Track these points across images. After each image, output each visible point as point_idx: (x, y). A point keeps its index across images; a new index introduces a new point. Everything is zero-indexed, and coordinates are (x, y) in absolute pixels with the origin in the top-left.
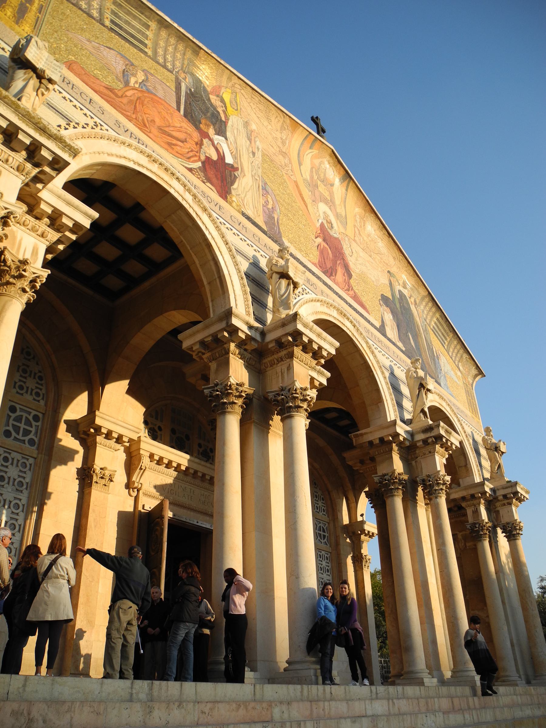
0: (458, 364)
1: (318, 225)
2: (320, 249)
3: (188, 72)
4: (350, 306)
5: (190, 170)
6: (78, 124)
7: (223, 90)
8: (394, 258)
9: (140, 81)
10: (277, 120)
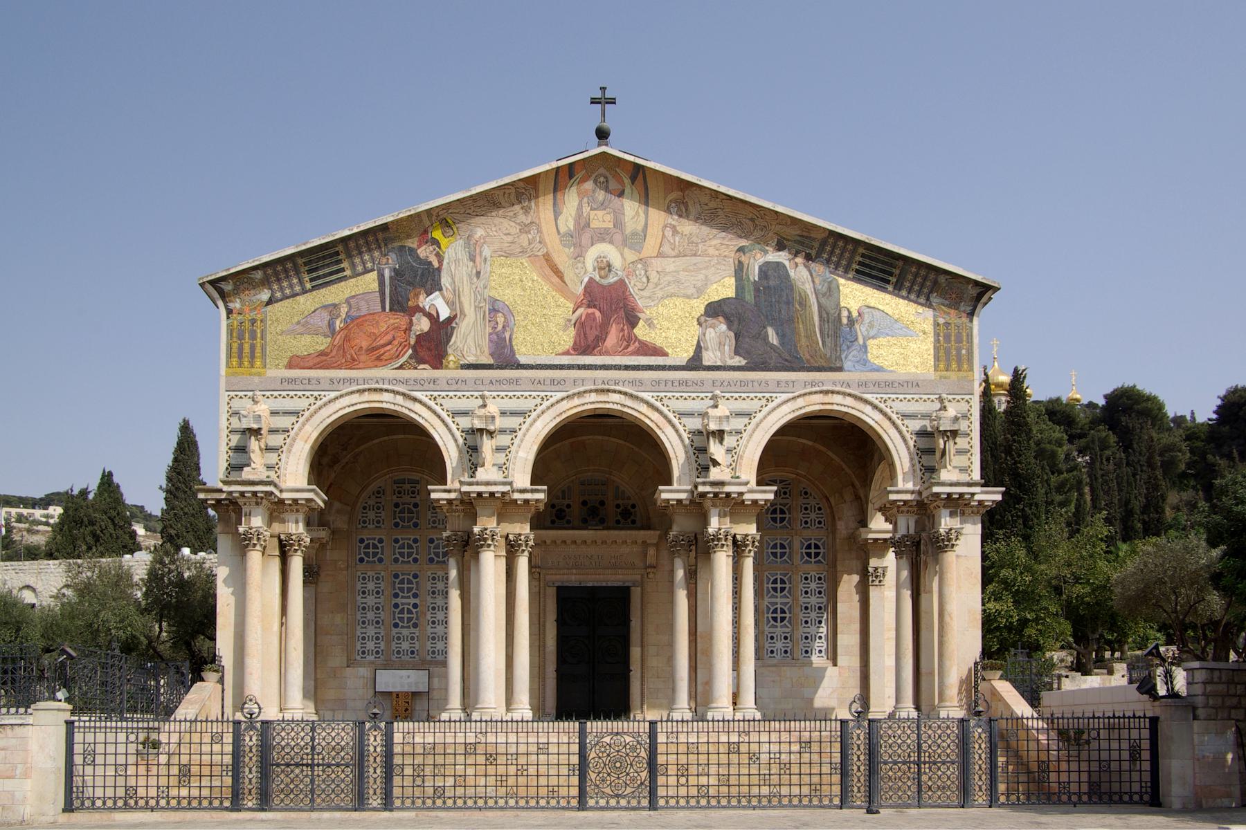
1: (580, 290)
2: (580, 323)
4: (627, 368)
5: (401, 367)
6: (304, 411)
8: (752, 220)
9: (344, 316)
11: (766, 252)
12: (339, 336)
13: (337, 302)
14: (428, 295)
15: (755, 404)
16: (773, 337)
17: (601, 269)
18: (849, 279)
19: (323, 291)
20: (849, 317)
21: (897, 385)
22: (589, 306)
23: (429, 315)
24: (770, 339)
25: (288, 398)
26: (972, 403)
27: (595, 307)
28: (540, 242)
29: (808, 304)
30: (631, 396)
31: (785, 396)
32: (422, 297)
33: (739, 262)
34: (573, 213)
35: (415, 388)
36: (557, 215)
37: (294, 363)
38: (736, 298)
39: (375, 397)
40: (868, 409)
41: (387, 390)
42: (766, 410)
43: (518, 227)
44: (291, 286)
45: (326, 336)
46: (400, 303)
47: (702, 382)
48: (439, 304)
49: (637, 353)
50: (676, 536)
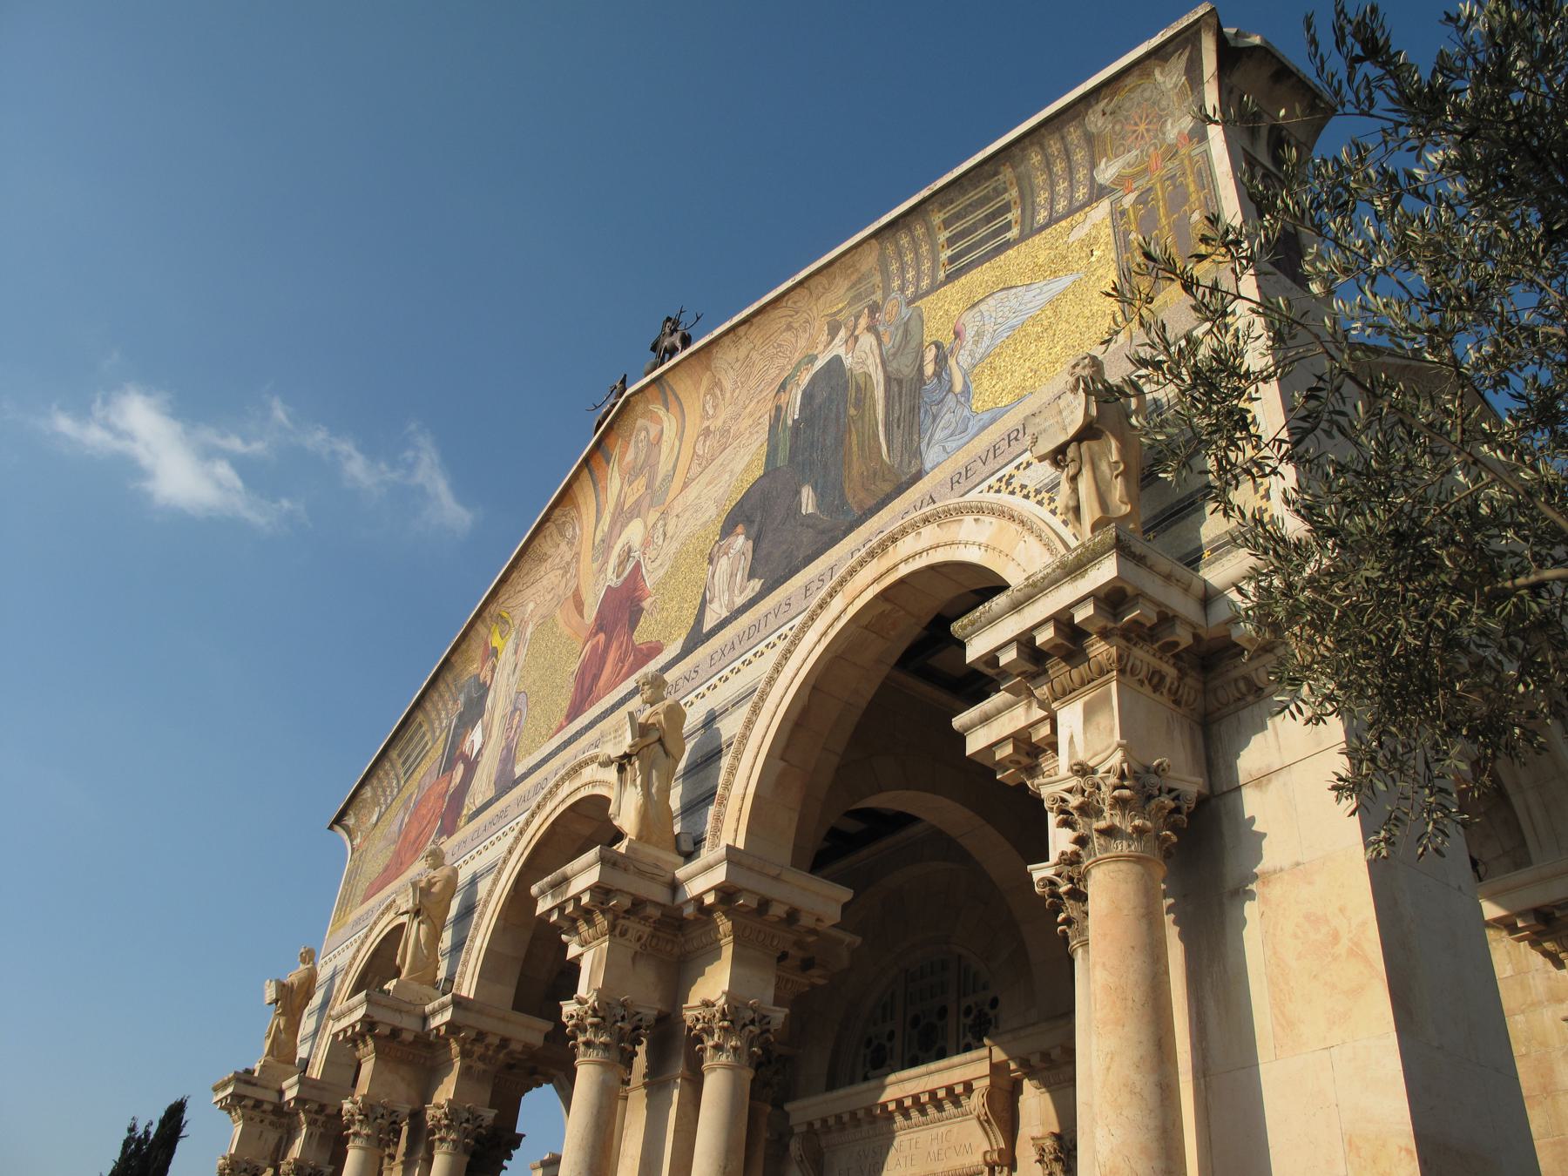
0: (1092, 179)
8: (789, 327)
10: (548, 539)
11: (816, 357)
16: (808, 501)
18: (943, 284)
22: (596, 634)
29: (868, 395)
33: (778, 409)
36: (598, 521)
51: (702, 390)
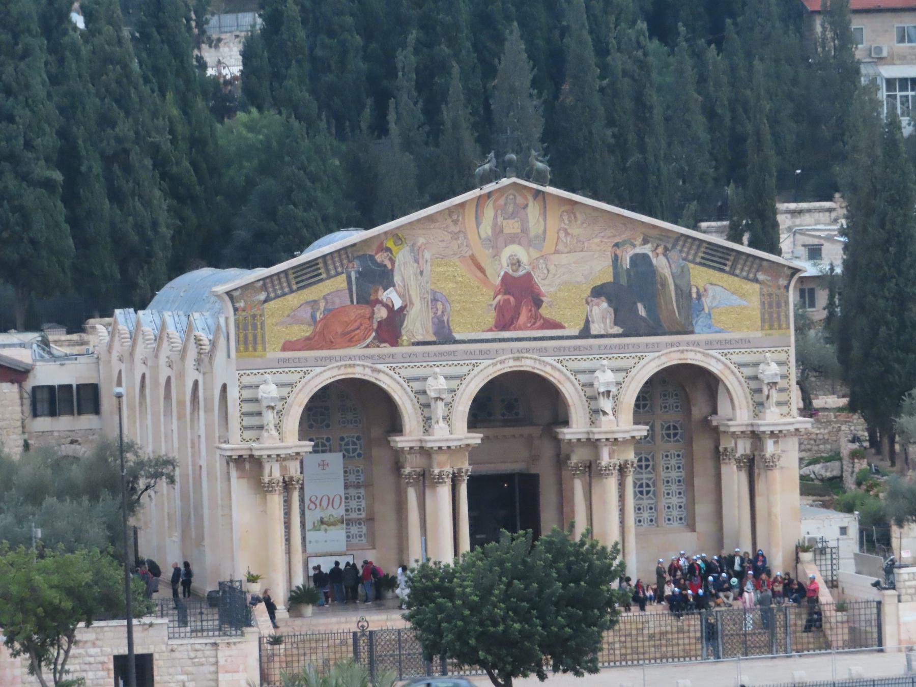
0: (755, 275)
1: (498, 281)
3: (354, 258)
4: (535, 339)
5: (367, 346)
7: (385, 242)
8: (624, 224)
9: (322, 308)
11: (634, 246)
12: (319, 326)
13: (316, 298)
14: (385, 289)
15: (631, 362)
16: (642, 311)
17: (513, 264)
19: (306, 291)
20: (698, 292)
21: (733, 342)
22: (505, 294)
23: (386, 306)
24: (640, 313)
25: (284, 374)
26: (789, 353)
27: (509, 294)
28: (467, 246)
30: (539, 360)
31: (652, 355)
32: (380, 292)
34: (491, 223)
35: (378, 362)
36: (478, 224)
37: (288, 346)
38: (614, 283)
39: (350, 370)
40: (713, 362)
41: (358, 365)
42: (638, 366)
43: (450, 236)
44: (282, 288)
45: (310, 325)
46: (366, 299)
47: (591, 347)
48: (393, 297)
49: (542, 327)
50: (575, 463)
51: (563, 208)
